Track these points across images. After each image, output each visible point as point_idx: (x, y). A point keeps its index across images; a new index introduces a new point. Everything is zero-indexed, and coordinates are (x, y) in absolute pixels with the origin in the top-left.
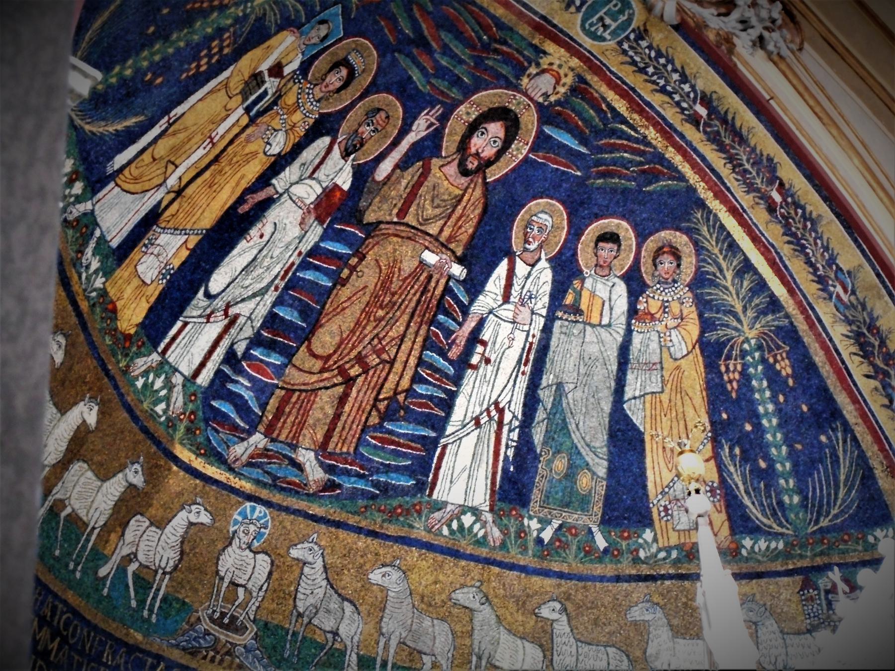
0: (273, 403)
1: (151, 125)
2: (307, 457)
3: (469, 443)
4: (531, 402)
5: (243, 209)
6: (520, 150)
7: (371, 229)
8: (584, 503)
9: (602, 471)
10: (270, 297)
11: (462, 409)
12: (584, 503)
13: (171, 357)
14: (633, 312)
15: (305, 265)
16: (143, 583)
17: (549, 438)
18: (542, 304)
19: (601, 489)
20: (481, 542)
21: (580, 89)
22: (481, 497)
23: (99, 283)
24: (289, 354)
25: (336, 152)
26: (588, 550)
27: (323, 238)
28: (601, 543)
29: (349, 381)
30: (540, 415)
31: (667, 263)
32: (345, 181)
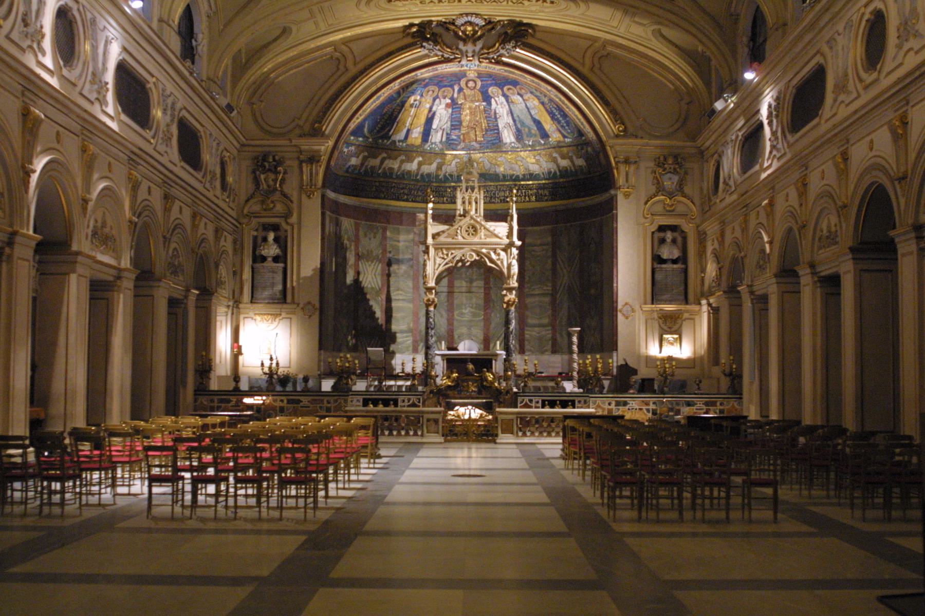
0: (462, 137)
1: (393, 125)
2: (474, 143)
3: (506, 131)
4: (514, 121)
5: (430, 116)
6: (479, 83)
7: (461, 104)
8: (535, 135)
9: (535, 128)
10: (449, 123)
11: (500, 126)
12: (535, 135)
13: (433, 141)
14: (524, 100)
15: (452, 115)
16: (451, 176)
17: (521, 126)
18: (505, 103)
19: (537, 132)
20: (518, 148)
21: (478, 74)
22: (513, 140)
23: (404, 144)
24: (460, 129)
25: (442, 100)
26: (540, 144)
27: (453, 109)
28: (543, 142)
29: (475, 128)
30: (517, 122)
31: (523, 91)
32: (448, 101)
